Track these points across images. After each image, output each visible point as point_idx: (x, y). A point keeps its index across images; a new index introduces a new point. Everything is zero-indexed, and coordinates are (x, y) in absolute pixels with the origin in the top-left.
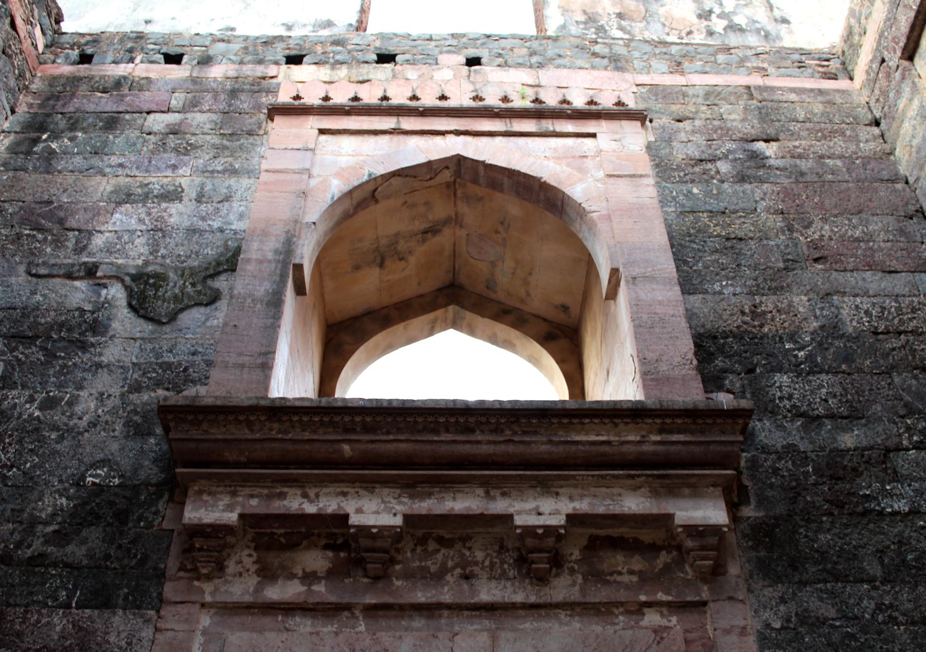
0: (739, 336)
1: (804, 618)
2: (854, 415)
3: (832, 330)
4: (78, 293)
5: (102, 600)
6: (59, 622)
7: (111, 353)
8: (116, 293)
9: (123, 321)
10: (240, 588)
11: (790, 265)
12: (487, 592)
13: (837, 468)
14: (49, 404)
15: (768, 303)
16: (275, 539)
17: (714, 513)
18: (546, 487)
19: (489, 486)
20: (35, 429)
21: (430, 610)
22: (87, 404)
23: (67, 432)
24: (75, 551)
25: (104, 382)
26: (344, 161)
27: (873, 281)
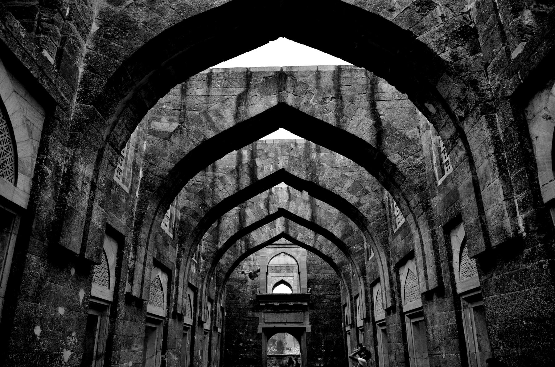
0: (313, 280)
1: (314, 313)
2: (323, 290)
3: (323, 279)
4: (243, 275)
5: (254, 311)
6: (251, 314)
7: (249, 284)
8: (247, 275)
9: (249, 279)
10: (265, 311)
11: (321, 268)
12: (286, 310)
13: (320, 297)
14: (244, 291)
15: (317, 275)
16: (267, 307)
17: (306, 304)
18: (292, 302)
19: (287, 302)
20: (243, 294)
21: (282, 312)
22: (248, 291)
23: (247, 294)
24: (250, 307)
25: (249, 288)
26: (270, 253)
27: (329, 271)
